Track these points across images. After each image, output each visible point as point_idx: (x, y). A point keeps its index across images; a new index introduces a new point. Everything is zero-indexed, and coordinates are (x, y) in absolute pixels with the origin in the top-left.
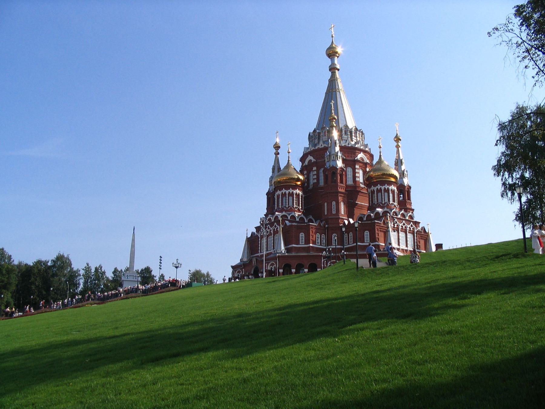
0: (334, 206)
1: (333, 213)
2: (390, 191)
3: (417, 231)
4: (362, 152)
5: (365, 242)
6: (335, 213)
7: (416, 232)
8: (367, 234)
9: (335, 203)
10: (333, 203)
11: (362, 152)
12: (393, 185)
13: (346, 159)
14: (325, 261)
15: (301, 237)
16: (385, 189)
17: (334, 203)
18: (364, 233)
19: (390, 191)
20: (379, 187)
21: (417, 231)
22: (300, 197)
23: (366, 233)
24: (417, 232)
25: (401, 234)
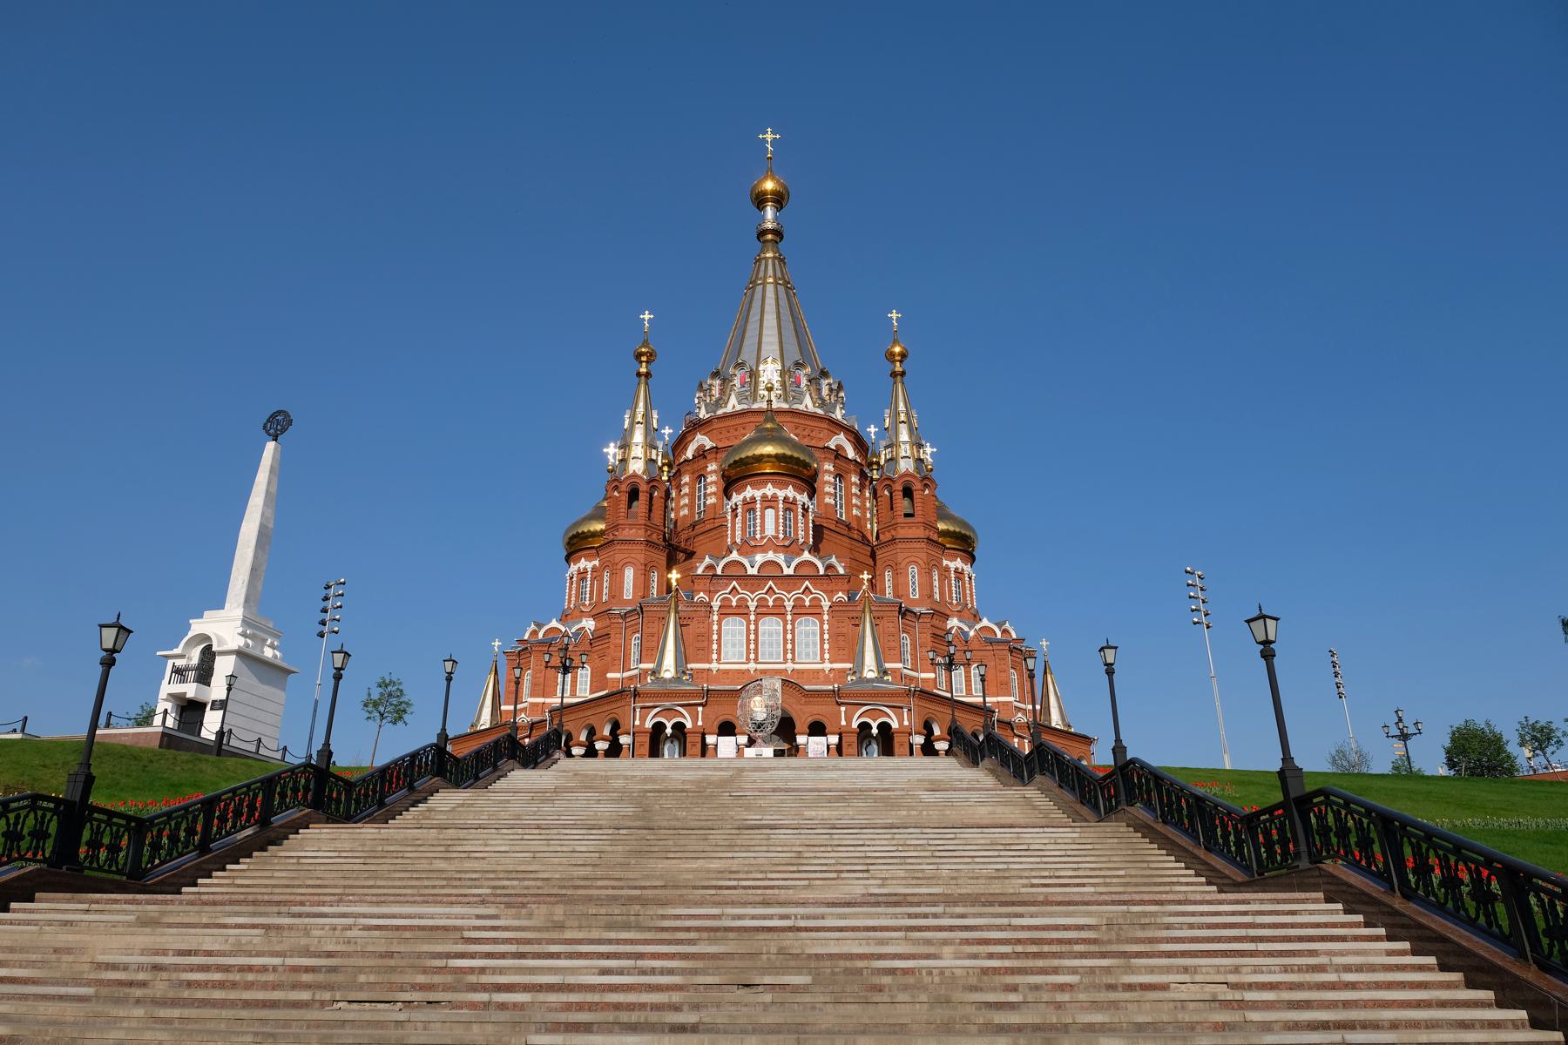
16: (764, 497)
20: (749, 492)
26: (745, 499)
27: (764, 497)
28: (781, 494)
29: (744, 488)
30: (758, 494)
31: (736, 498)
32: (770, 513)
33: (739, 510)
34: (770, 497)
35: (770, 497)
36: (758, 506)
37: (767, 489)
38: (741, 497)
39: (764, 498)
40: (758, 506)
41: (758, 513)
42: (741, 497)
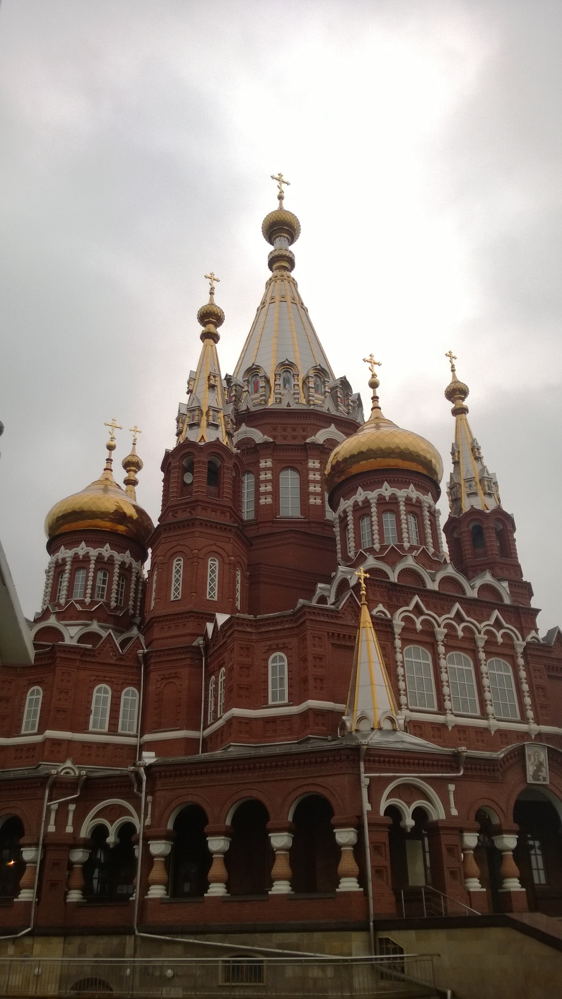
0: (178, 572)
1: (172, 598)
2: (402, 503)
3: (528, 643)
4: (333, 425)
5: (270, 702)
6: (180, 597)
7: (520, 650)
8: (278, 664)
9: (182, 563)
10: (175, 563)
11: (333, 425)
12: (415, 485)
13: (274, 442)
14: (72, 807)
15: (31, 700)
16: (381, 498)
17: (178, 564)
18: (266, 660)
19: (402, 503)
20: (360, 495)
21: (528, 643)
22: (117, 570)
23: (274, 661)
24: (525, 649)
25: (451, 661)
26: (356, 504)
27: (381, 498)
28: (401, 494)
29: (354, 491)
30: (373, 495)
31: (346, 504)
32: (389, 518)
33: (350, 518)
34: (387, 498)
35: (387, 498)
36: (374, 509)
37: (383, 489)
38: (351, 502)
39: (381, 499)
40: (374, 509)
41: (375, 518)
42: (351, 502)
